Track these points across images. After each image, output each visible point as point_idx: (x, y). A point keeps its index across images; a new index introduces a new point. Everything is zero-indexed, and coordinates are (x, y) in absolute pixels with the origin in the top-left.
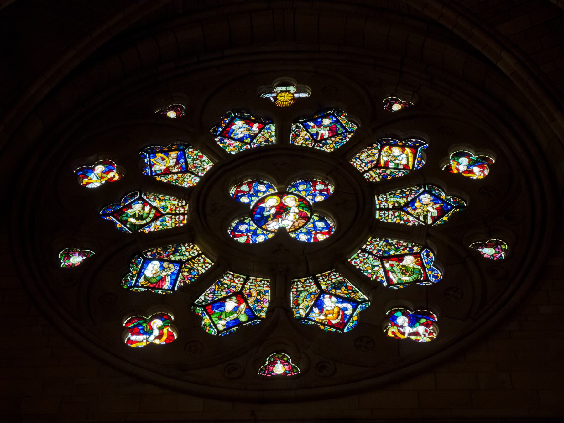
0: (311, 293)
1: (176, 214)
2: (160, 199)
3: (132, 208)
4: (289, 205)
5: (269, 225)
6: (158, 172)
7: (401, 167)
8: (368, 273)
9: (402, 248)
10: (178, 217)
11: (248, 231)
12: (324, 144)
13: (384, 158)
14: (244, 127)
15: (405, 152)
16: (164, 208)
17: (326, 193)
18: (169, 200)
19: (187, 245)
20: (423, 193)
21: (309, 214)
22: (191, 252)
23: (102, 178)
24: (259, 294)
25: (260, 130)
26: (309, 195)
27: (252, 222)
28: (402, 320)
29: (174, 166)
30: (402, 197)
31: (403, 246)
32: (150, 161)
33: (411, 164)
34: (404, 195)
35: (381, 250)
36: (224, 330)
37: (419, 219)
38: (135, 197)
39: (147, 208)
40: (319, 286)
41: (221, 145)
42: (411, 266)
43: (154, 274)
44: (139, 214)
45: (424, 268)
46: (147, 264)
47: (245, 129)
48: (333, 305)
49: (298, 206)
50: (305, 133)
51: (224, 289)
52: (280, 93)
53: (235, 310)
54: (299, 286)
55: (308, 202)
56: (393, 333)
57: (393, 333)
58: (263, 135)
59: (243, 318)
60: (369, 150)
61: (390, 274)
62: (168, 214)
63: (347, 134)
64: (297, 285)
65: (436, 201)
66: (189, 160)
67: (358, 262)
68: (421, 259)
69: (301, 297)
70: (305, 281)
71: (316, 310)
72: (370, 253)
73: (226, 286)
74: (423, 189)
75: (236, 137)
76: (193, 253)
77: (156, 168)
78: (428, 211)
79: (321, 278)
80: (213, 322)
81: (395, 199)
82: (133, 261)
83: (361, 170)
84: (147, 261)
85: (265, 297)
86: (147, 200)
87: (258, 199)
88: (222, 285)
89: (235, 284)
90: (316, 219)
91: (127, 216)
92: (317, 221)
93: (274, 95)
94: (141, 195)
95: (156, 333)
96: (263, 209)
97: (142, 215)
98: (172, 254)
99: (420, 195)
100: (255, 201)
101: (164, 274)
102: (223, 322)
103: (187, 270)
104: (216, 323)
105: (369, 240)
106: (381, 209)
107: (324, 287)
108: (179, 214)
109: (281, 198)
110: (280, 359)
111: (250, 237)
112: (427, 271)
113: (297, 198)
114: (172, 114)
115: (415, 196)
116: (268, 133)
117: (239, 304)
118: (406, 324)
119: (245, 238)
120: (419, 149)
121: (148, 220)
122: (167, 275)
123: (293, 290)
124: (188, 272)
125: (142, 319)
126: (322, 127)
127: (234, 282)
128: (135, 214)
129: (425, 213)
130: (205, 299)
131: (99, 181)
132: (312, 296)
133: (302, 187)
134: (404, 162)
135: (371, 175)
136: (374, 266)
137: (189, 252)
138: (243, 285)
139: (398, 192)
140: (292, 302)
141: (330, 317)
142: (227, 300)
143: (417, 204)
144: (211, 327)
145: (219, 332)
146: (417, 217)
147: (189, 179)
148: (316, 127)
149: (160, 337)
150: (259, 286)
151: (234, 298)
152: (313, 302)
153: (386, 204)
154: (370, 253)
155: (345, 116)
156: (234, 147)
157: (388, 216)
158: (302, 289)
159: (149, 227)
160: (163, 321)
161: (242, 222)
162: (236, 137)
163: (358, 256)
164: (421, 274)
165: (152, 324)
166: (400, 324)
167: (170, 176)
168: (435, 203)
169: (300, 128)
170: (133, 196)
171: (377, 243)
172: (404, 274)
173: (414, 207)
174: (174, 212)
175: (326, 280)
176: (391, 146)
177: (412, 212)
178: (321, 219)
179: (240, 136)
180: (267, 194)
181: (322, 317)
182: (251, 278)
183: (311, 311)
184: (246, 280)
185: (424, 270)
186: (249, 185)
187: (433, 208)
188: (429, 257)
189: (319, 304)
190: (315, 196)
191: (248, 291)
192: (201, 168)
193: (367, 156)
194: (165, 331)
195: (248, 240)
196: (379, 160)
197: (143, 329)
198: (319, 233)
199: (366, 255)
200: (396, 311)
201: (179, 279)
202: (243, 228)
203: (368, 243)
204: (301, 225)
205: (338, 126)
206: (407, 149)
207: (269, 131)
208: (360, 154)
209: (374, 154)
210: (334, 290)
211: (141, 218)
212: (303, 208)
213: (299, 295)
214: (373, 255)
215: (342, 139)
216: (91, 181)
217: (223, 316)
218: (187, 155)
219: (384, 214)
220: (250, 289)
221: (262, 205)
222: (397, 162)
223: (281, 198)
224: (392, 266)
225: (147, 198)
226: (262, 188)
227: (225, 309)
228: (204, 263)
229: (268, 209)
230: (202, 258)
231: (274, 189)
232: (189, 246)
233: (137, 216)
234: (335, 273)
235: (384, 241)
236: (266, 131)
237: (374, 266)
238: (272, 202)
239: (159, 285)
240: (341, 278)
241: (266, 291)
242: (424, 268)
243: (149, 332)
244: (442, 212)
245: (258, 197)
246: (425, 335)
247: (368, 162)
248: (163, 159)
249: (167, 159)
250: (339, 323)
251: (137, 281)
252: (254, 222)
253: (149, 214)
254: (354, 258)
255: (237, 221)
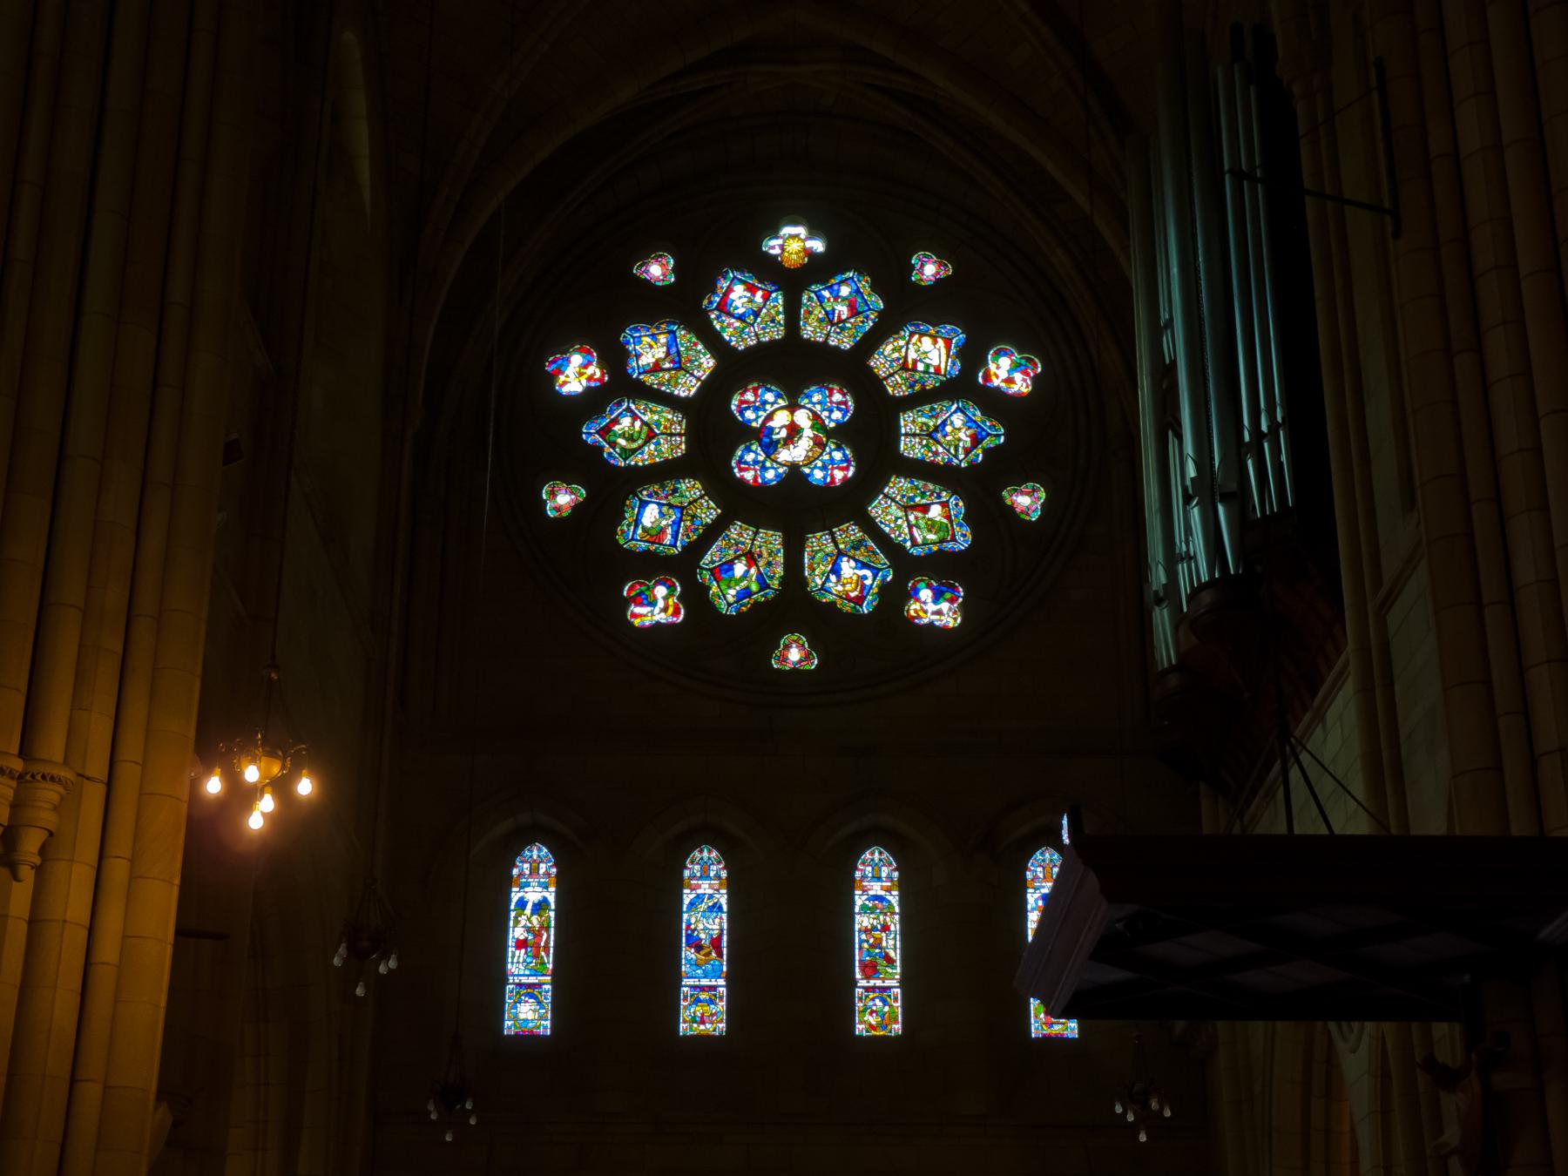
0: (827, 555)
1: (671, 435)
2: (651, 411)
3: (620, 424)
4: (802, 426)
5: (779, 454)
6: (647, 368)
7: (932, 370)
8: (890, 527)
9: (928, 494)
10: (673, 439)
11: (756, 462)
12: (843, 329)
13: (912, 355)
14: (745, 297)
15: (937, 346)
16: (658, 424)
17: (843, 407)
18: (662, 411)
19: (687, 481)
20: (955, 412)
21: (824, 439)
22: (692, 493)
23: (581, 374)
24: (770, 555)
25: (766, 297)
26: (824, 410)
27: (759, 449)
28: (925, 594)
29: (664, 359)
30: (932, 416)
31: (930, 490)
32: (635, 350)
33: (943, 367)
34: (934, 413)
35: (905, 495)
36: (735, 602)
37: (948, 451)
38: (622, 406)
39: (638, 424)
40: (836, 546)
41: (718, 327)
42: (938, 519)
43: (653, 523)
44: (629, 434)
45: (951, 521)
46: (644, 508)
47: (746, 299)
48: (851, 571)
49: (812, 427)
50: (819, 309)
51: (732, 546)
52: (787, 239)
53: (745, 576)
54: (815, 544)
55: (823, 421)
56: (916, 611)
57: (916, 611)
58: (768, 311)
59: (754, 587)
60: (895, 340)
61: (915, 529)
62: (662, 434)
63: (869, 313)
64: (812, 543)
65: (970, 424)
66: (682, 349)
67: (880, 512)
68: (949, 510)
69: (817, 559)
70: (821, 537)
71: (833, 578)
72: (893, 500)
73: (732, 541)
74: (956, 405)
75: (736, 311)
76: (695, 494)
77: (644, 361)
78: (960, 440)
79: (838, 533)
80: (721, 590)
81: (924, 420)
82: (628, 502)
83: (884, 372)
84: (644, 504)
85: (777, 559)
86: (636, 411)
87: (765, 414)
88: (729, 540)
89: (744, 540)
90: (833, 447)
91: (615, 435)
92: (835, 450)
93: (780, 242)
94: (628, 403)
95: (661, 604)
96: (772, 429)
97: (632, 435)
98: (672, 494)
99: (951, 415)
100: (763, 418)
101: (664, 523)
102: (733, 592)
103: (689, 518)
104: (725, 592)
105: (893, 480)
106: (907, 435)
107: (842, 546)
108: (675, 435)
109: (792, 413)
110: (795, 641)
111: (759, 472)
112: (955, 526)
113: (811, 415)
114: (655, 270)
115: (947, 415)
116: (775, 306)
117: (749, 567)
118: (929, 600)
119: (752, 473)
120: (954, 341)
121: (640, 442)
122: (668, 525)
123: (807, 549)
124: (690, 520)
125: (644, 584)
126: (840, 300)
127: (742, 536)
128: (624, 433)
129: (957, 443)
130: (712, 558)
131: (577, 380)
132: (829, 559)
133: (816, 397)
134: (936, 363)
135: (896, 380)
136: (897, 518)
137: (690, 492)
138: (753, 540)
139: (927, 408)
140: (806, 565)
141: (848, 587)
142: (736, 561)
143: (948, 429)
144: (720, 598)
145: (729, 605)
146: (947, 447)
147: (684, 381)
148: (832, 300)
149: (665, 610)
150: (771, 543)
151: (743, 558)
152: (830, 566)
153: (912, 427)
154: (893, 500)
155: (867, 281)
156: (735, 329)
157: (914, 445)
158: (818, 548)
159: (642, 453)
160: (668, 588)
161: (748, 450)
162: (736, 311)
163: (879, 503)
164: (948, 532)
165: (655, 591)
166: (923, 599)
167: (661, 375)
168: (969, 428)
169: (812, 302)
170: (619, 404)
171: (901, 484)
172: (930, 531)
173: (944, 433)
174: (669, 432)
175: (844, 536)
176: (922, 335)
177: (942, 440)
178: (839, 448)
179: (741, 311)
180: (776, 406)
181: (840, 588)
182: (761, 530)
183: (828, 578)
184: (756, 533)
185: (952, 526)
186: (755, 391)
187: (967, 436)
188: (957, 505)
189: (836, 570)
190: (831, 411)
191: (758, 550)
192: (696, 363)
193: (893, 350)
194: (671, 602)
195: (755, 478)
196: (906, 357)
197: (646, 599)
198: (836, 468)
199: (889, 502)
200: (919, 581)
201: (681, 530)
202: (750, 457)
203: (891, 485)
204: (816, 456)
205: (859, 300)
206: (939, 340)
207: (776, 304)
208: (884, 347)
209: (902, 347)
210: (853, 551)
211: (631, 439)
212: (818, 430)
213: (814, 557)
214: (897, 502)
215: (863, 322)
216: (568, 379)
217: (733, 584)
218: (678, 340)
219: (911, 441)
220: (760, 547)
221: (771, 424)
222: (927, 361)
223: (792, 413)
224: (916, 518)
225: (636, 408)
226: (770, 397)
227: (733, 575)
228: (708, 508)
229: (777, 430)
230: (707, 501)
231: (784, 400)
232: (689, 482)
233: (627, 436)
234: (854, 527)
235: (909, 483)
236: (772, 304)
237: (897, 518)
238: (781, 419)
239: (659, 540)
240: (861, 534)
241: (779, 551)
242: (951, 521)
243: (653, 604)
244: (976, 440)
245: (765, 410)
246: (948, 614)
247: (893, 360)
248: (651, 347)
249: (655, 346)
250: (857, 596)
251: (634, 532)
252: (762, 450)
253: (640, 432)
254: (876, 507)
255: (742, 447)
